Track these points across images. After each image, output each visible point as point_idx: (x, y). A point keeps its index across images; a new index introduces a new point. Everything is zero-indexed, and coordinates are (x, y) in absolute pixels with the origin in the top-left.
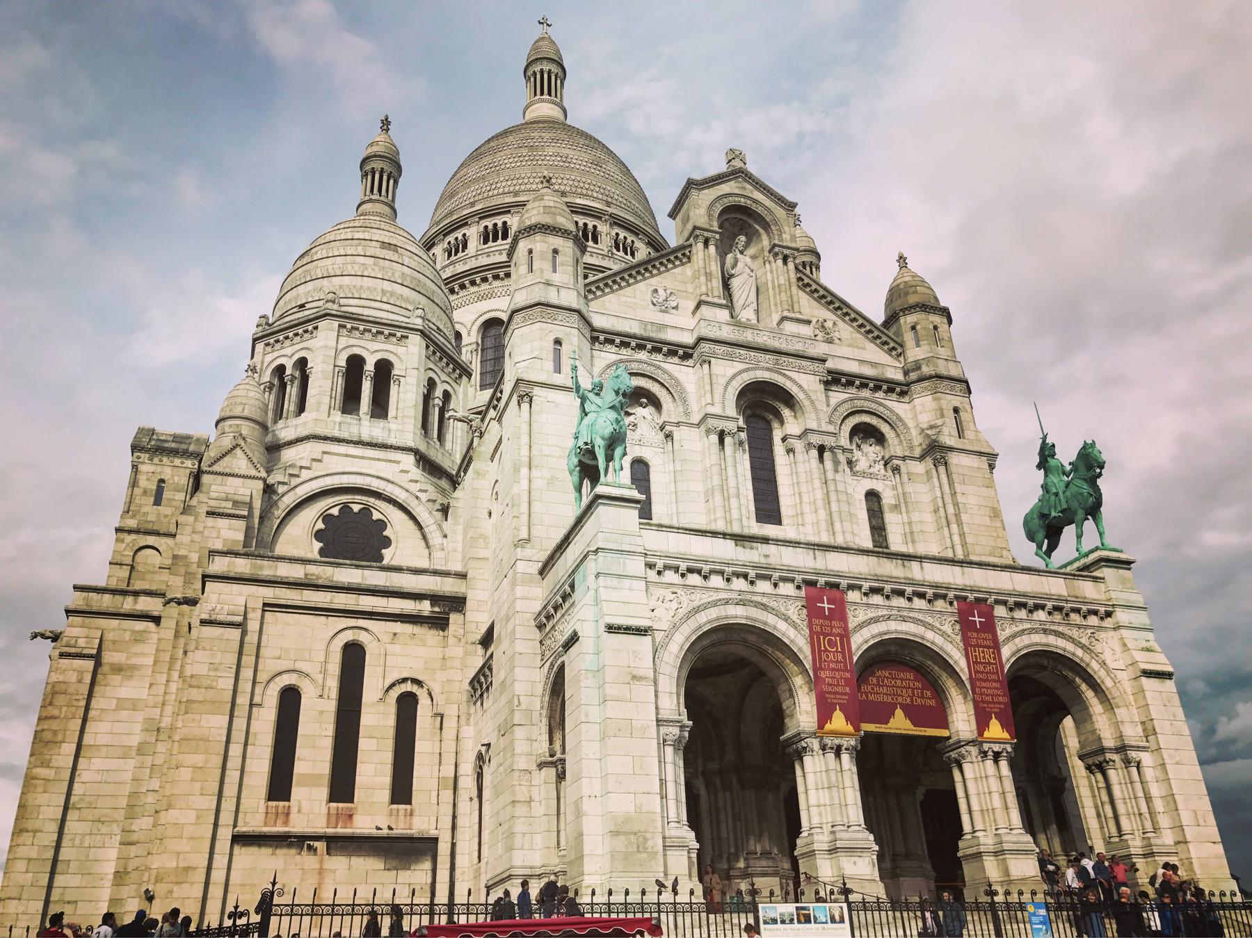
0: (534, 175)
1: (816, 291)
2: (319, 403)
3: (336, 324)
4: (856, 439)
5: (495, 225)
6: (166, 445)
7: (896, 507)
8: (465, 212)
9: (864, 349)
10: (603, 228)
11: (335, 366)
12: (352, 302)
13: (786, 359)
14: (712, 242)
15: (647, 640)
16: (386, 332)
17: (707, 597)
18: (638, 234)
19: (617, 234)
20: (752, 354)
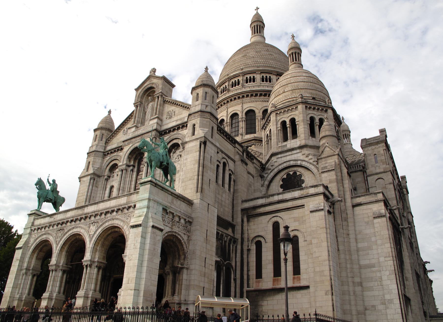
1: (169, 101)
4: (173, 150)
10: (240, 78)
13: (144, 136)
14: (138, 106)
15: (21, 250)
17: (40, 235)
18: (256, 73)
19: (247, 78)
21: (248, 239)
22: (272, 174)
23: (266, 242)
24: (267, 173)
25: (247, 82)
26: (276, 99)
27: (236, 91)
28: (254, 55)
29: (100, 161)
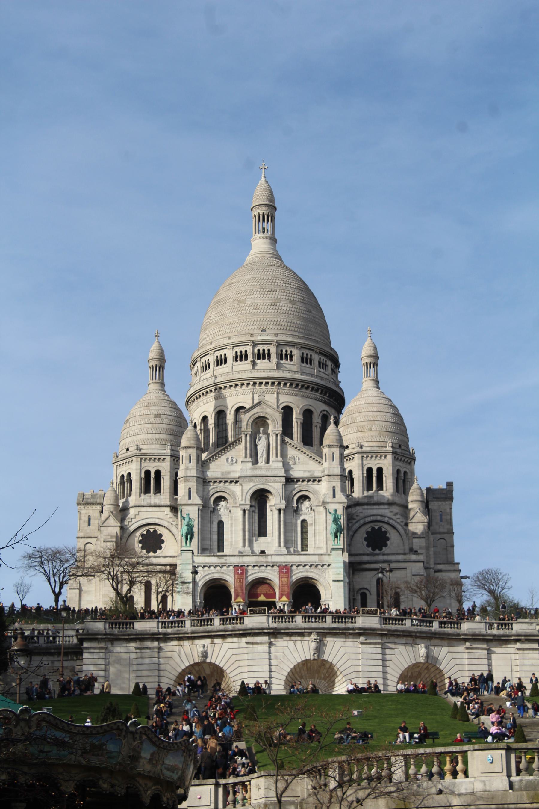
0: (240, 321)
2: (136, 492)
3: (139, 459)
5: (221, 355)
6: (89, 501)
7: (311, 524)
8: (209, 347)
9: (308, 464)
11: (140, 476)
12: (144, 447)
16: (157, 458)
19: (282, 351)
20: (258, 479)
21: (353, 589)
22: (357, 525)
23: (370, 594)
24: (351, 523)
25: (282, 359)
26: (359, 434)
27: (270, 372)
28: (288, 309)
29: (202, 489)
